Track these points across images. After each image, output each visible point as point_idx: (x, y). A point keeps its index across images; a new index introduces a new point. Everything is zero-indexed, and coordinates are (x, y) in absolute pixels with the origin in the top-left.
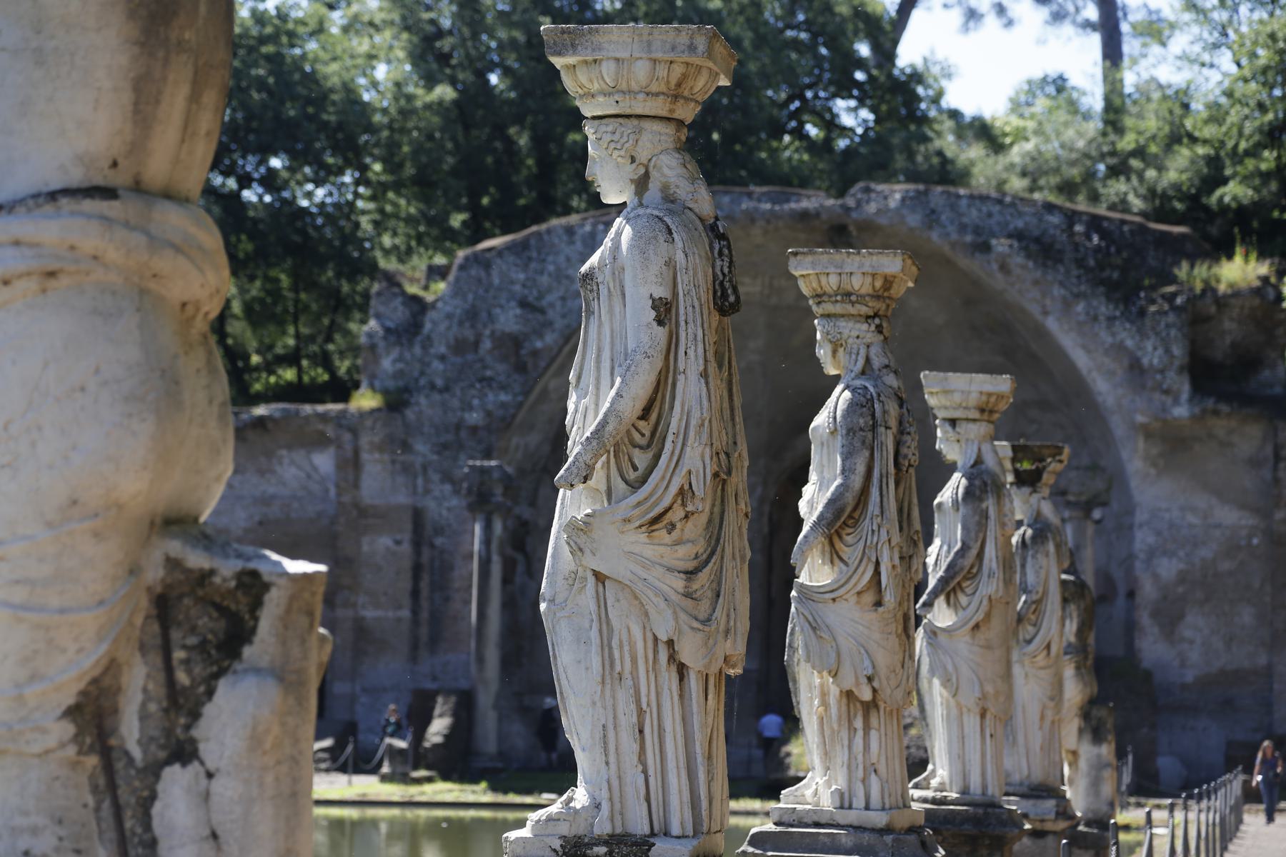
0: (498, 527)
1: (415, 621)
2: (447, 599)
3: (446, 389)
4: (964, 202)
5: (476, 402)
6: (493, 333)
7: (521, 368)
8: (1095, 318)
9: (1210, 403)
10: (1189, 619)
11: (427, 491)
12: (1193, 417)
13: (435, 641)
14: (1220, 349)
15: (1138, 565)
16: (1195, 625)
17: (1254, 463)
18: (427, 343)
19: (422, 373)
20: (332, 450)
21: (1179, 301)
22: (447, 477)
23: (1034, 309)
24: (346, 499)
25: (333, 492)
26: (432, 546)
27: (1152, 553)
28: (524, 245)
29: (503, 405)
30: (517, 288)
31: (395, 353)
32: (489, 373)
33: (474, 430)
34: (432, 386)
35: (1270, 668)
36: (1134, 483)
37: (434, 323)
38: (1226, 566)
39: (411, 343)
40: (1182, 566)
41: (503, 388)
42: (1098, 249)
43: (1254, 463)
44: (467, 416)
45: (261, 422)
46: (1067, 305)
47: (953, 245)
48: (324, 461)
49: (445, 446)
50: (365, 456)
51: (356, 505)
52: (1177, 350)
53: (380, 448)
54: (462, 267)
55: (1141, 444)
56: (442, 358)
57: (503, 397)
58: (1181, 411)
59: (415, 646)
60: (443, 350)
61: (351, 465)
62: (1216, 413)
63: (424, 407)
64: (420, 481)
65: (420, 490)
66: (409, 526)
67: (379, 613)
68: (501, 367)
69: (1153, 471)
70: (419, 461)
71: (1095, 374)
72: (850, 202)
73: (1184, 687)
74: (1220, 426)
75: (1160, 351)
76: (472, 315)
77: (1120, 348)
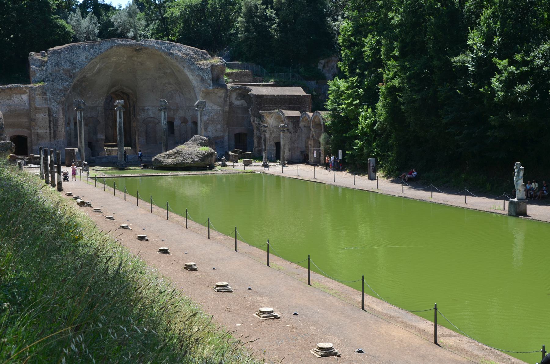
1: (50, 133)
3: (53, 81)
7: (70, 77)
13: (55, 137)
16: (210, 128)
17: (220, 97)
22: (55, 101)
23: (182, 68)
33: (61, 90)
34: (49, 80)
38: (215, 117)
45: (10, 88)
48: (25, 97)
53: (39, 95)
57: (67, 83)
58: (211, 88)
68: (65, 76)
70: (48, 97)
77: (199, 75)
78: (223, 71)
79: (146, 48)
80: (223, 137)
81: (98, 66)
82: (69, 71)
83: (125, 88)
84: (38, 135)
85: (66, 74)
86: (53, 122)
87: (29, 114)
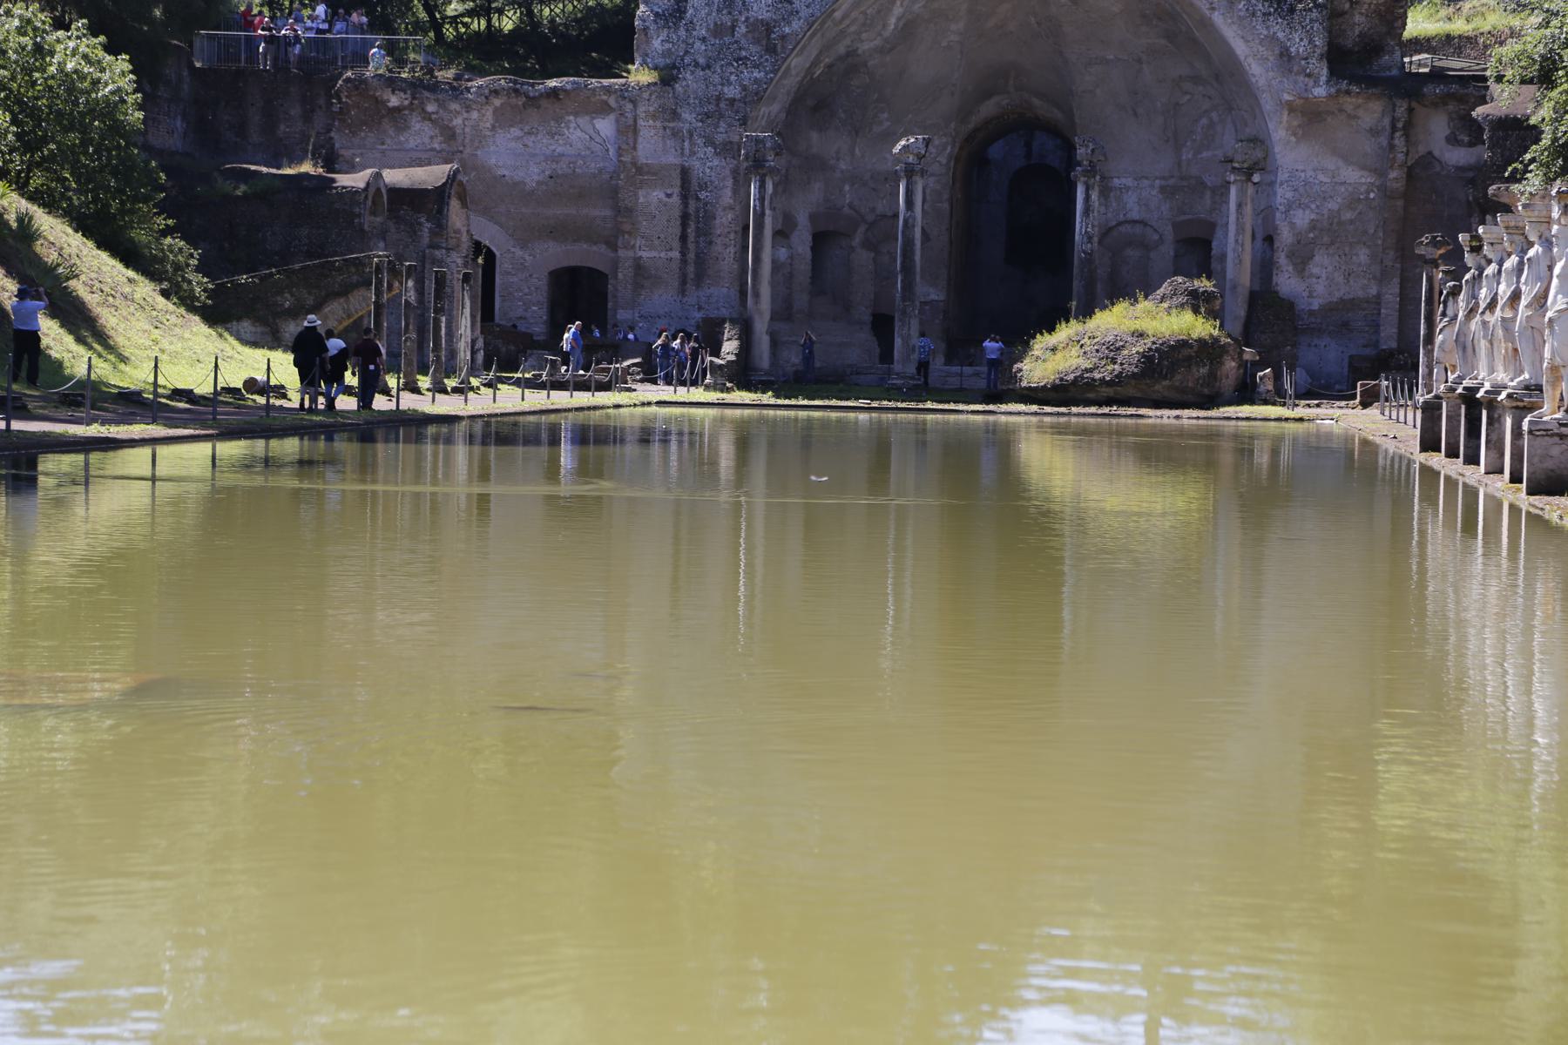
1: (684, 261)
2: (711, 243)
3: (708, 67)
5: (733, 78)
6: (747, 19)
7: (771, 49)
8: (1254, 15)
9: (1344, 85)
10: (1317, 258)
11: (693, 153)
12: (1330, 96)
13: (700, 278)
14: (1350, 39)
15: (1278, 215)
16: (1322, 264)
17: (1374, 132)
18: (690, 27)
19: (687, 52)
20: (612, 117)
22: (709, 142)
26: (698, 199)
27: (1289, 207)
31: (664, 34)
32: (744, 53)
33: (732, 101)
34: (697, 65)
35: (1379, 296)
37: (696, 9)
38: (1348, 215)
39: (677, 28)
40: (1313, 216)
44: (726, 90)
45: (554, 92)
48: (605, 126)
49: (708, 115)
50: (641, 122)
51: (634, 164)
53: (654, 117)
56: (704, 40)
58: (1320, 91)
59: (684, 282)
61: (629, 131)
62: (1348, 93)
63: (690, 81)
65: (687, 152)
66: (678, 182)
67: (654, 254)
68: (753, 49)
69: (1293, 139)
71: (1250, 60)
73: (1312, 313)
74: (1349, 103)
75: (1305, 42)
77: (1273, 38)
80: (1377, 301)
81: (898, 10)
82: (768, 27)
83: (1036, 102)
84: (638, 266)
85: (757, 42)
87: (614, 189)
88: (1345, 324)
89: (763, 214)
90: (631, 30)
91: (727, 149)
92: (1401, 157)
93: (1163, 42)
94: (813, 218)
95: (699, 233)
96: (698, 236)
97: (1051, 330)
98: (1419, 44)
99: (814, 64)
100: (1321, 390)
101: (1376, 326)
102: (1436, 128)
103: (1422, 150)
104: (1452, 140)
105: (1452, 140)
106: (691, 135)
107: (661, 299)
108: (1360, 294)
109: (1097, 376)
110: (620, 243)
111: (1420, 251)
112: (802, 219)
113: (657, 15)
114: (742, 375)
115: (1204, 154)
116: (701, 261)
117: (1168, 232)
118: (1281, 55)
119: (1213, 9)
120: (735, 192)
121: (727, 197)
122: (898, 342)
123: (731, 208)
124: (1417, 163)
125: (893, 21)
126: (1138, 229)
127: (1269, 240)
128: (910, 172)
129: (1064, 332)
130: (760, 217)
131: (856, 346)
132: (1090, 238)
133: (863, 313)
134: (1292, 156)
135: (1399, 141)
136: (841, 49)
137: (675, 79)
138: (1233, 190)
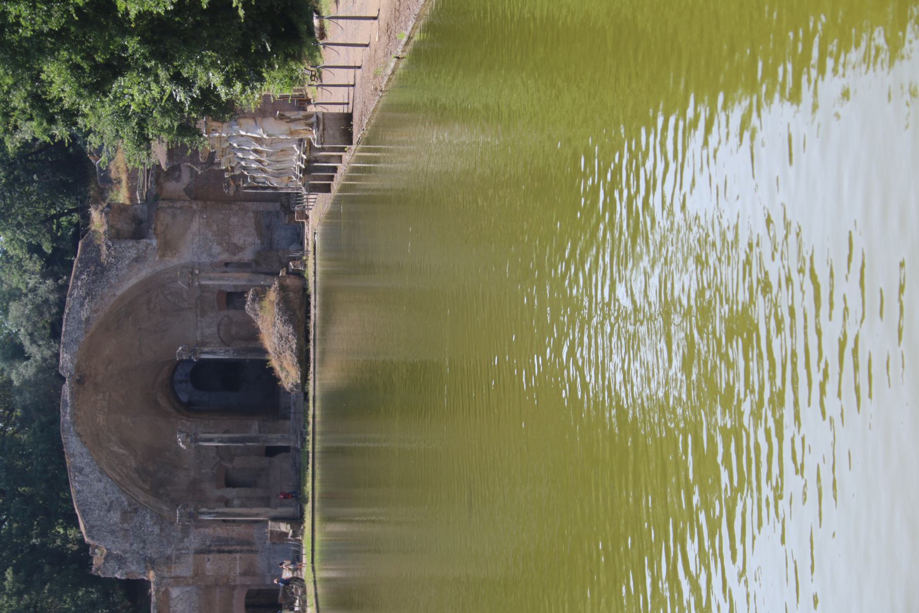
0: (204, 510)
1: (241, 551)
3: (144, 542)
4: (68, 328)
7: (136, 511)
10: (236, 241)
11: (187, 548)
12: (157, 238)
13: (249, 543)
17: (174, 216)
18: (125, 552)
19: (138, 553)
20: (170, 589)
21: (110, 244)
22: (182, 540)
23: (113, 299)
24: (191, 581)
25: (188, 589)
27: (211, 255)
28: (83, 512)
29: (151, 517)
30: (102, 514)
33: (162, 530)
34: (143, 548)
35: (254, 212)
36: (183, 262)
38: (215, 228)
41: (144, 517)
42: (88, 275)
43: (174, 216)
46: (111, 287)
47: (86, 332)
48: (175, 592)
50: (173, 575)
51: (193, 578)
52: (130, 244)
53: (170, 568)
54: (93, 538)
55: (167, 259)
56: (131, 545)
59: (252, 551)
60: (128, 545)
62: (155, 229)
63: (151, 552)
64: (183, 552)
66: (202, 556)
72: (67, 375)
73: (262, 243)
74: (160, 228)
76: (112, 532)
77: (129, 266)
78: (122, 208)
79: (78, 368)
80: (256, 213)
81: (116, 449)
82: (124, 513)
84: (245, 574)
86: (222, 547)
88: (268, 227)
89: (217, 513)
90: (128, 580)
91: (186, 531)
92: (186, 204)
93: (130, 318)
94: (218, 487)
95: (227, 544)
96: (229, 545)
97: (272, 369)
98: (132, 198)
99: (142, 489)
100: (298, 237)
101: (269, 213)
102: (172, 187)
103: (183, 193)
104: (178, 179)
105: (178, 179)
106: (178, 550)
107: (260, 562)
108: (253, 220)
109: (294, 346)
110: (233, 584)
111: (232, 193)
112: (220, 493)
113: (119, 568)
114: (296, 520)
115: (185, 296)
116: (241, 542)
117: (224, 313)
118: (137, 262)
119: (114, 295)
120: (206, 527)
121: (209, 531)
122: (279, 444)
123: (214, 528)
124: (189, 195)
125: (121, 451)
126: (222, 327)
127: (227, 264)
128: (197, 440)
129: (274, 363)
130: (218, 514)
131: (281, 463)
132: (227, 351)
133: (265, 461)
134: (187, 254)
135: (178, 205)
136: (135, 476)
137: (151, 558)
138: (204, 282)
